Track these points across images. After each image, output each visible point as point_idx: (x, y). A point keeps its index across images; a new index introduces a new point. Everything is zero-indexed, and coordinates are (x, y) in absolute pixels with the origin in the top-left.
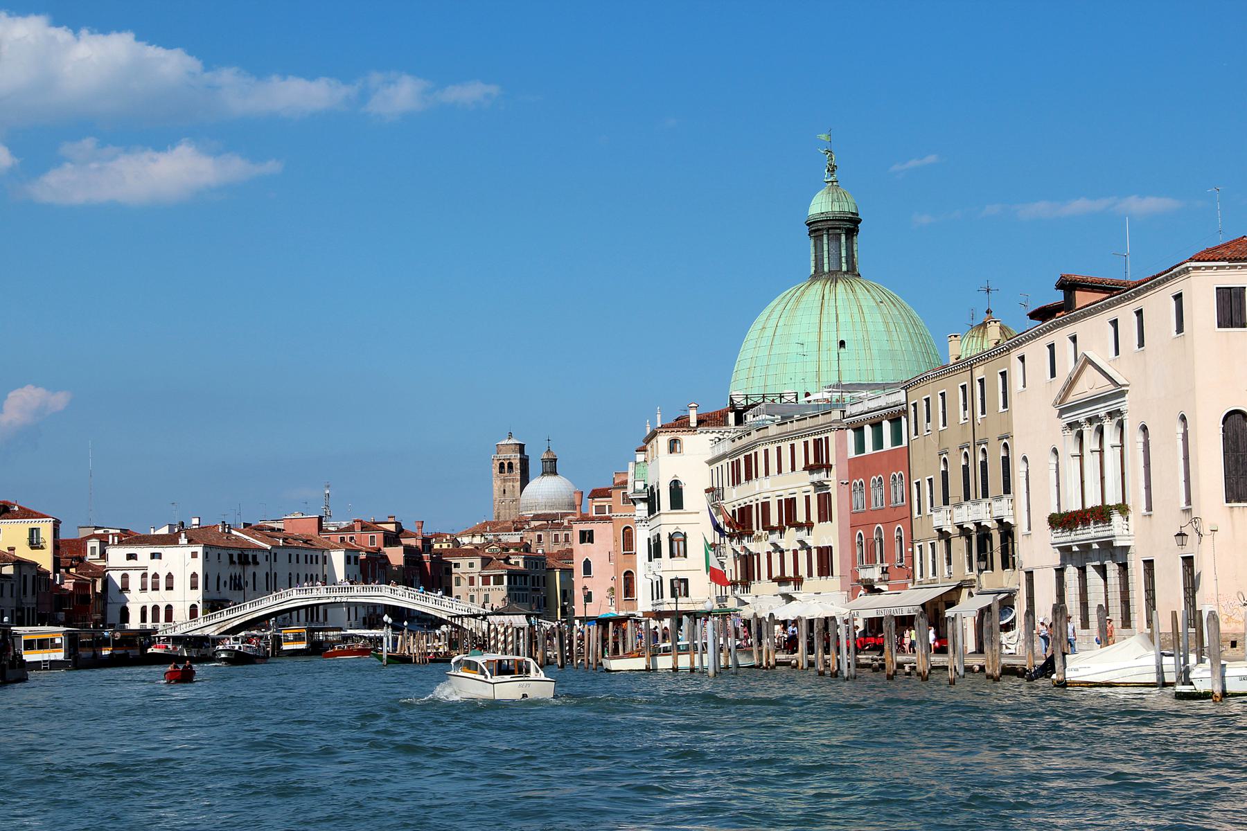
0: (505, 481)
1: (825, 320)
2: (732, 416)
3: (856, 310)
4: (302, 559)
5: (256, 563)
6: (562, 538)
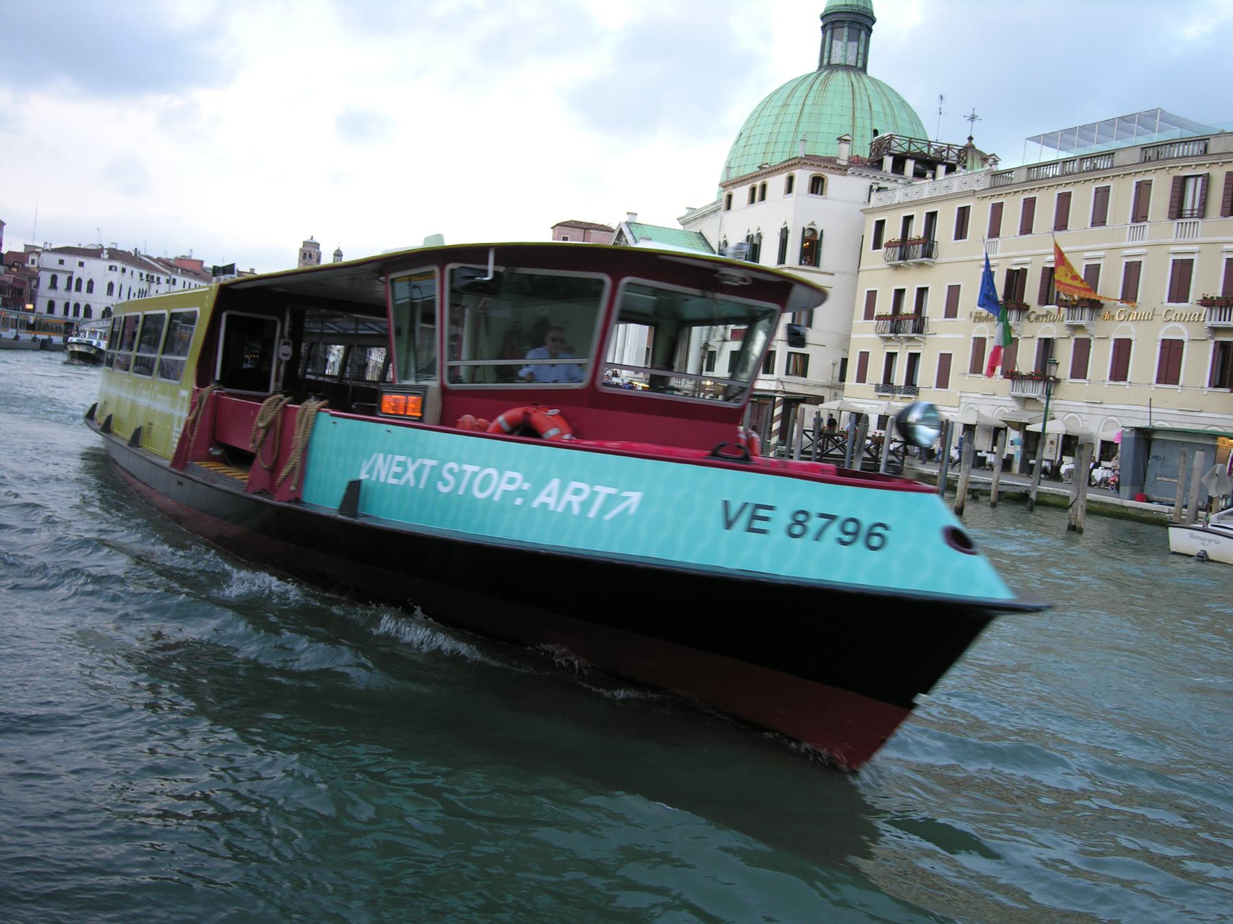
1: (858, 106)
2: (888, 162)
3: (885, 103)
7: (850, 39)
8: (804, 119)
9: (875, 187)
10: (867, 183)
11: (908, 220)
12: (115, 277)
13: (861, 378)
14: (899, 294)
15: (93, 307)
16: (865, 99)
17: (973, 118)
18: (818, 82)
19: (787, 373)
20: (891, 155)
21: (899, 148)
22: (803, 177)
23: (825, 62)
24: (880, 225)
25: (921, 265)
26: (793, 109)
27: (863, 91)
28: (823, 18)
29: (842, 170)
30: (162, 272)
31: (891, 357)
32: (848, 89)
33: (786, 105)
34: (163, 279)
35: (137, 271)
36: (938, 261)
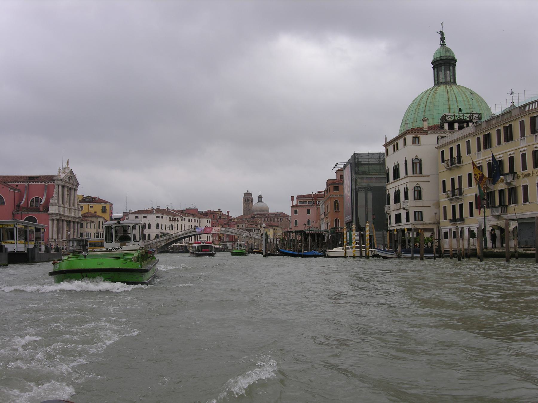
0: (246, 204)
1: (450, 99)
2: (446, 126)
3: (464, 96)
4: (193, 221)
5: (178, 221)
6: (266, 220)
7: (445, 71)
8: (427, 109)
9: (440, 137)
10: (435, 136)
11: (451, 149)
12: (160, 221)
13: (445, 218)
14: (453, 180)
15: (151, 234)
16: (453, 96)
17: (512, 93)
18: (432, 92)
19: (415, 220)
20: (446, 122)
21: (450, 119)
22: (409, 138)
23: (436, 82)
24: (443, 152)
25: (457, 167)
26: (422, 106)
27: (452, 92)
28: (432, 63)
29: (426, 133)
30: (179, 216)
31: (454, 207)
32: (445, 93)
33: (419, 105)
34: (180, 219)
35: (168, 218)
36: (463, 164)
